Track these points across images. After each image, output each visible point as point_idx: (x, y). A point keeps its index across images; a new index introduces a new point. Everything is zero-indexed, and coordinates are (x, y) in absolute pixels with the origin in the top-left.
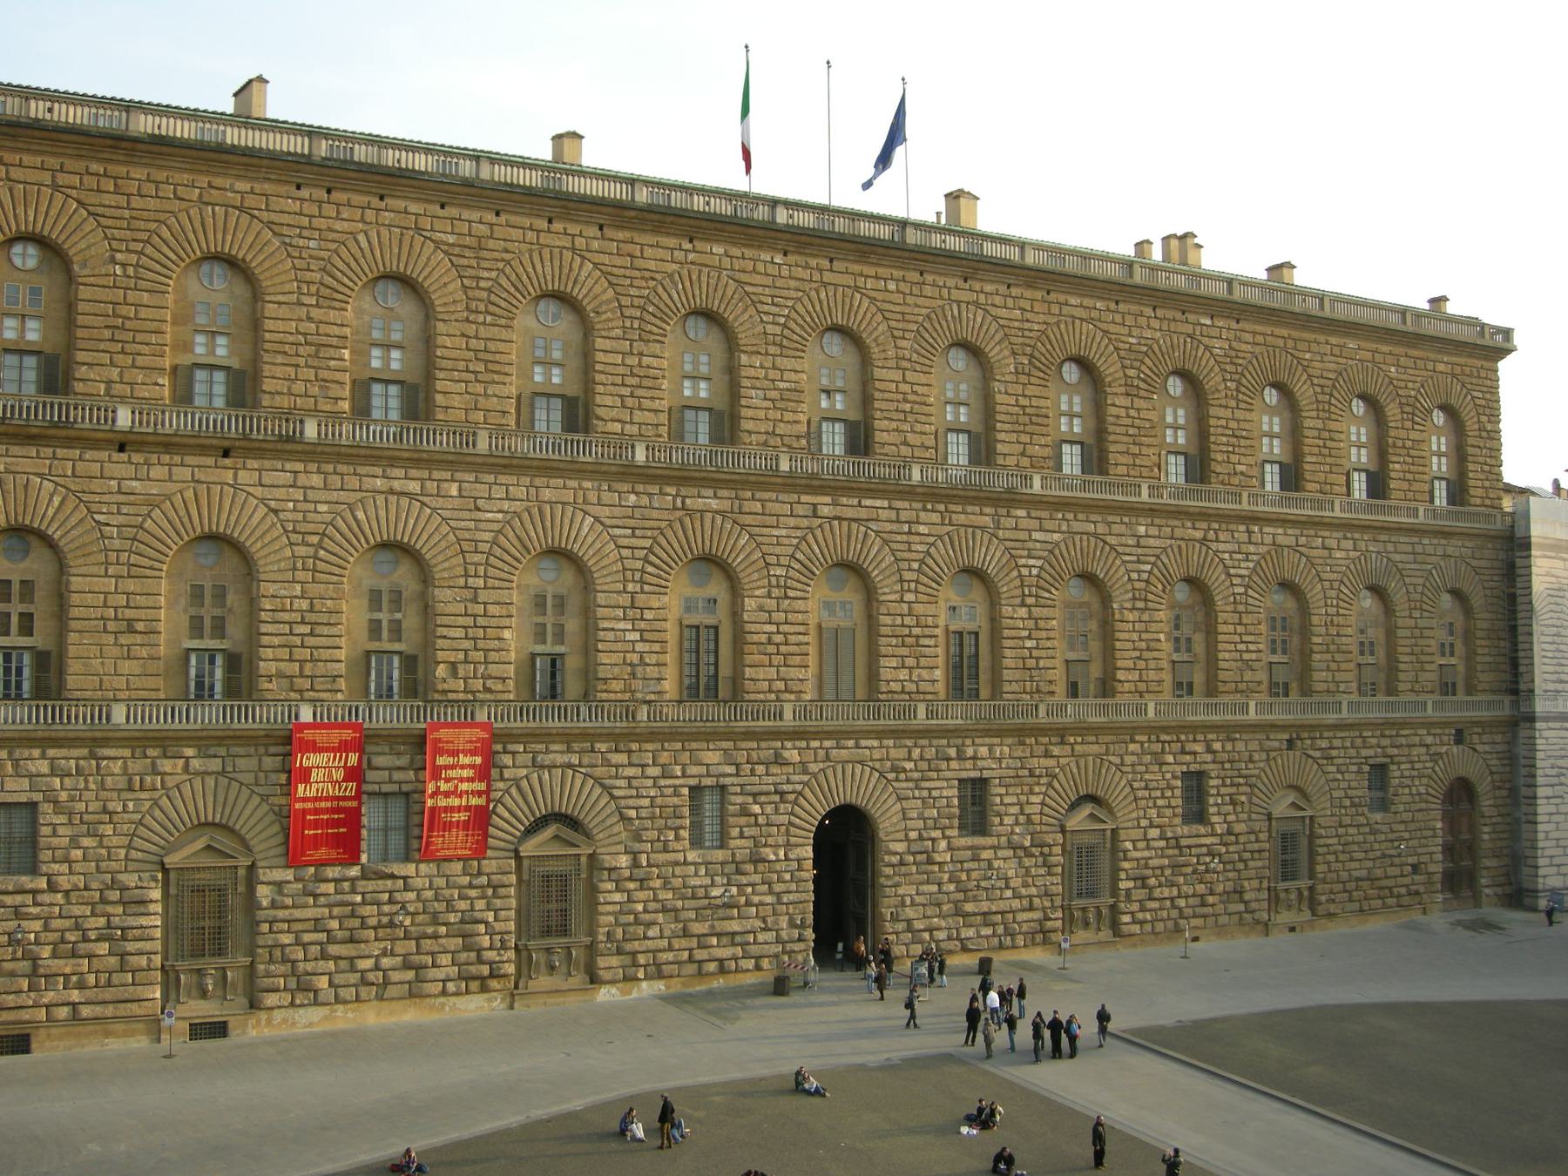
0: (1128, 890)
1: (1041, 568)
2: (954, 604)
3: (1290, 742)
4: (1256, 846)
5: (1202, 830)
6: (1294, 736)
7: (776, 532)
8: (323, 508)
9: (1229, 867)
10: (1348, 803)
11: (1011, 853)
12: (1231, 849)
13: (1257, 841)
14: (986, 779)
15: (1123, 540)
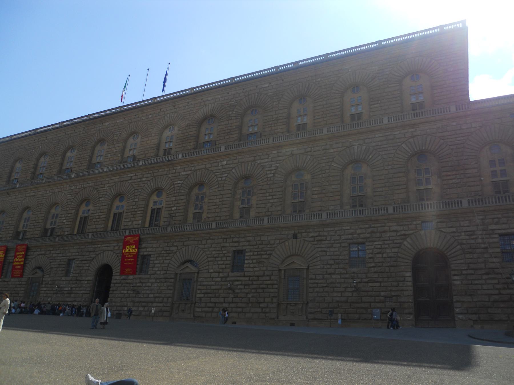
0: (200, 298)
1: (182, 183)
2: (155, 201)
3: (295, 236)
4: (269, 282)
5: (239, 274)
6: (297, 232)
7: (103, 189)
8: (19, 202)
9: (253, 291)
10: (332, 262)
11: (154, 281)
12: (254, 283)
13: (270, 280)
14: (150, 255)
15: (216, 168)
